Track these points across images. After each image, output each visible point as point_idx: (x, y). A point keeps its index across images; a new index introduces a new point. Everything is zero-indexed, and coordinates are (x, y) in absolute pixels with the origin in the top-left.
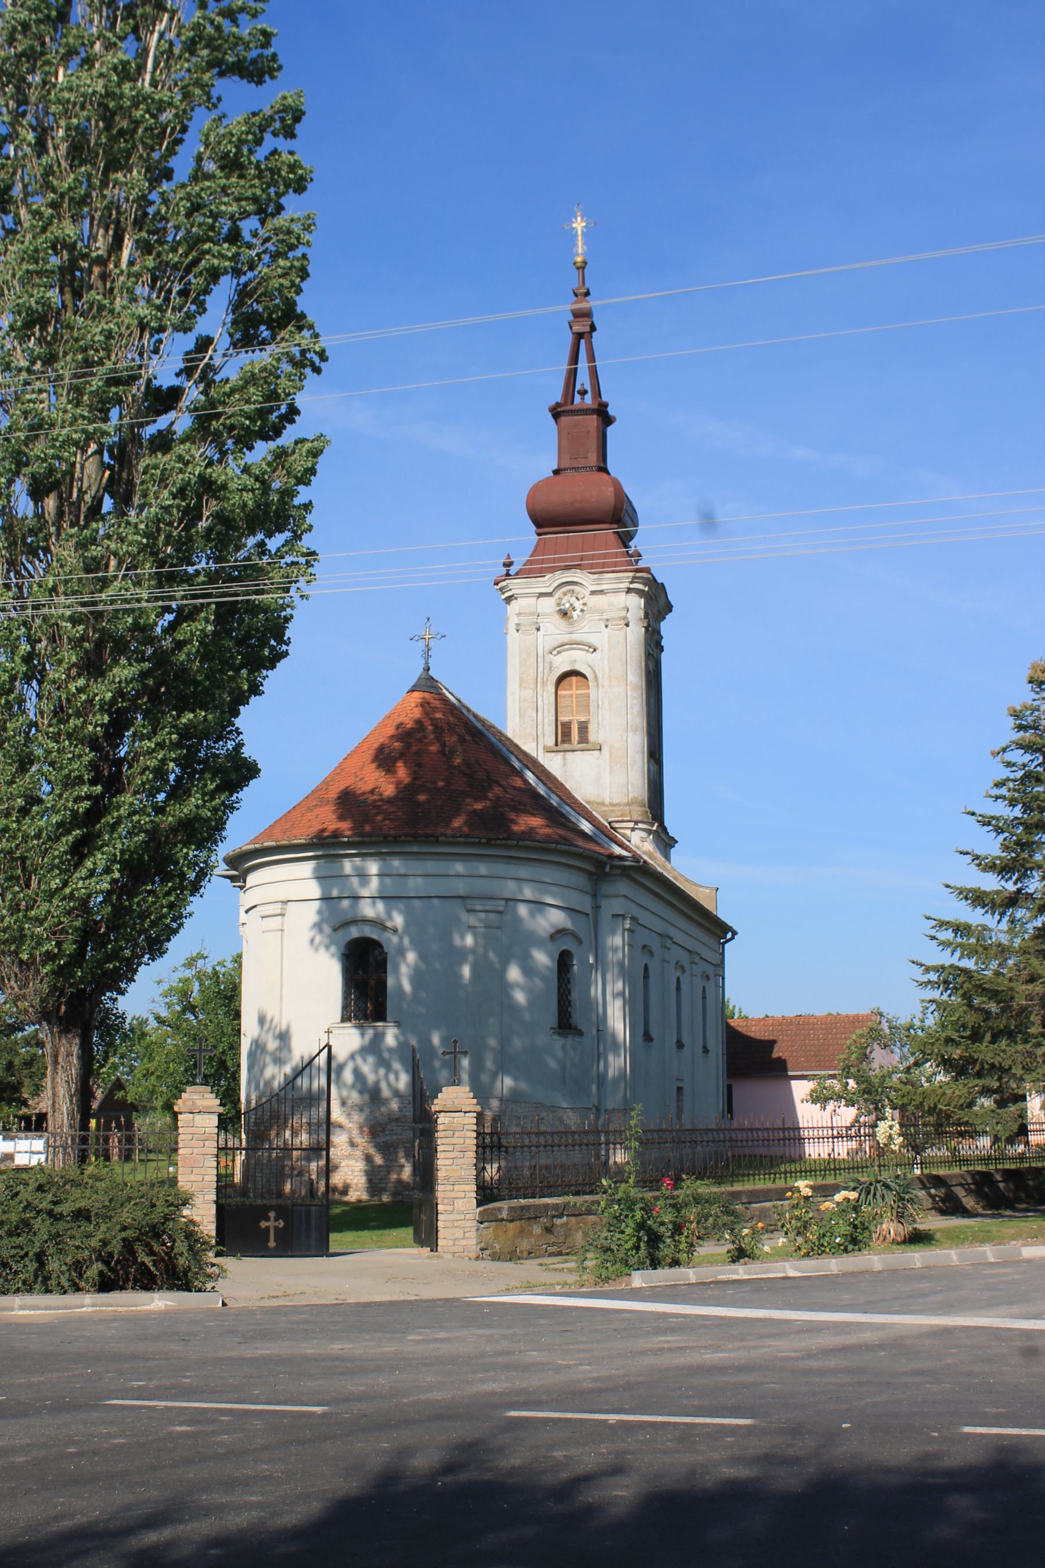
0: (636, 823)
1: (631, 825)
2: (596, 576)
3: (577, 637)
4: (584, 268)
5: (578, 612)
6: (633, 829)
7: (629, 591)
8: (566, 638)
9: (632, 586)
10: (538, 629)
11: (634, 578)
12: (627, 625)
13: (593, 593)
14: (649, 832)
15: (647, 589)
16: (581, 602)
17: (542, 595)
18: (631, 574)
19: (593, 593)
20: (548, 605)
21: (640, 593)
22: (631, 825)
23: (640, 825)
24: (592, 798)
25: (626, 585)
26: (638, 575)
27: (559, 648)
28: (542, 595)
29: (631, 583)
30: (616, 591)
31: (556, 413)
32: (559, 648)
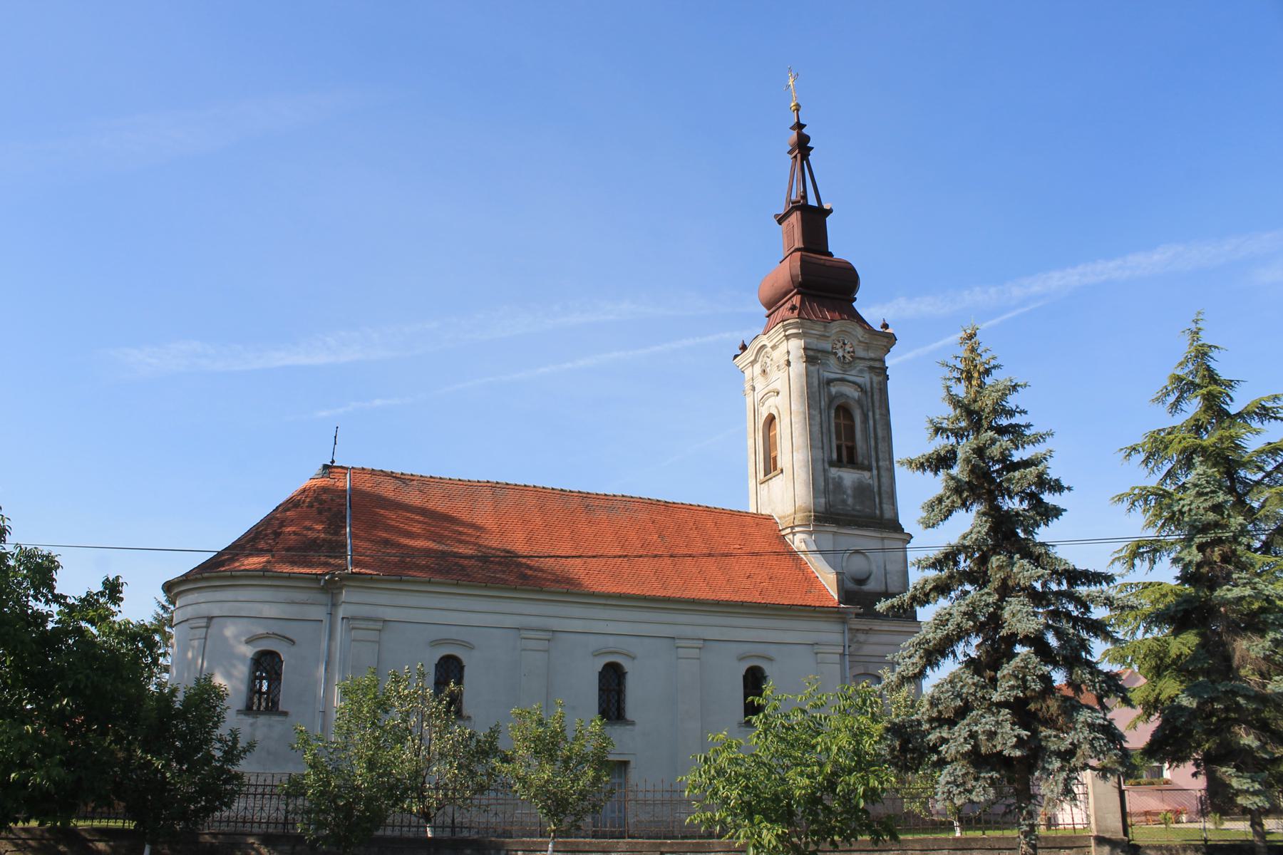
0: (792, 528)
1: (789, 530)
3: (770, 388)
6: (794, 534)
7: (787, 337)
8: (766, 391)
10: (754, 389)
12: (789, 363)
13: (774, 347)
14: (810, 533)
17: (753, 363)
19: (774, 347)
20: (758, 368)
21: (795, 335)
22: (789, 530)
23: (797, 529)
24: (782, 514)
27: (763, 400)
28: (753, 363)
31: (780, 222)
32: (763, 400)
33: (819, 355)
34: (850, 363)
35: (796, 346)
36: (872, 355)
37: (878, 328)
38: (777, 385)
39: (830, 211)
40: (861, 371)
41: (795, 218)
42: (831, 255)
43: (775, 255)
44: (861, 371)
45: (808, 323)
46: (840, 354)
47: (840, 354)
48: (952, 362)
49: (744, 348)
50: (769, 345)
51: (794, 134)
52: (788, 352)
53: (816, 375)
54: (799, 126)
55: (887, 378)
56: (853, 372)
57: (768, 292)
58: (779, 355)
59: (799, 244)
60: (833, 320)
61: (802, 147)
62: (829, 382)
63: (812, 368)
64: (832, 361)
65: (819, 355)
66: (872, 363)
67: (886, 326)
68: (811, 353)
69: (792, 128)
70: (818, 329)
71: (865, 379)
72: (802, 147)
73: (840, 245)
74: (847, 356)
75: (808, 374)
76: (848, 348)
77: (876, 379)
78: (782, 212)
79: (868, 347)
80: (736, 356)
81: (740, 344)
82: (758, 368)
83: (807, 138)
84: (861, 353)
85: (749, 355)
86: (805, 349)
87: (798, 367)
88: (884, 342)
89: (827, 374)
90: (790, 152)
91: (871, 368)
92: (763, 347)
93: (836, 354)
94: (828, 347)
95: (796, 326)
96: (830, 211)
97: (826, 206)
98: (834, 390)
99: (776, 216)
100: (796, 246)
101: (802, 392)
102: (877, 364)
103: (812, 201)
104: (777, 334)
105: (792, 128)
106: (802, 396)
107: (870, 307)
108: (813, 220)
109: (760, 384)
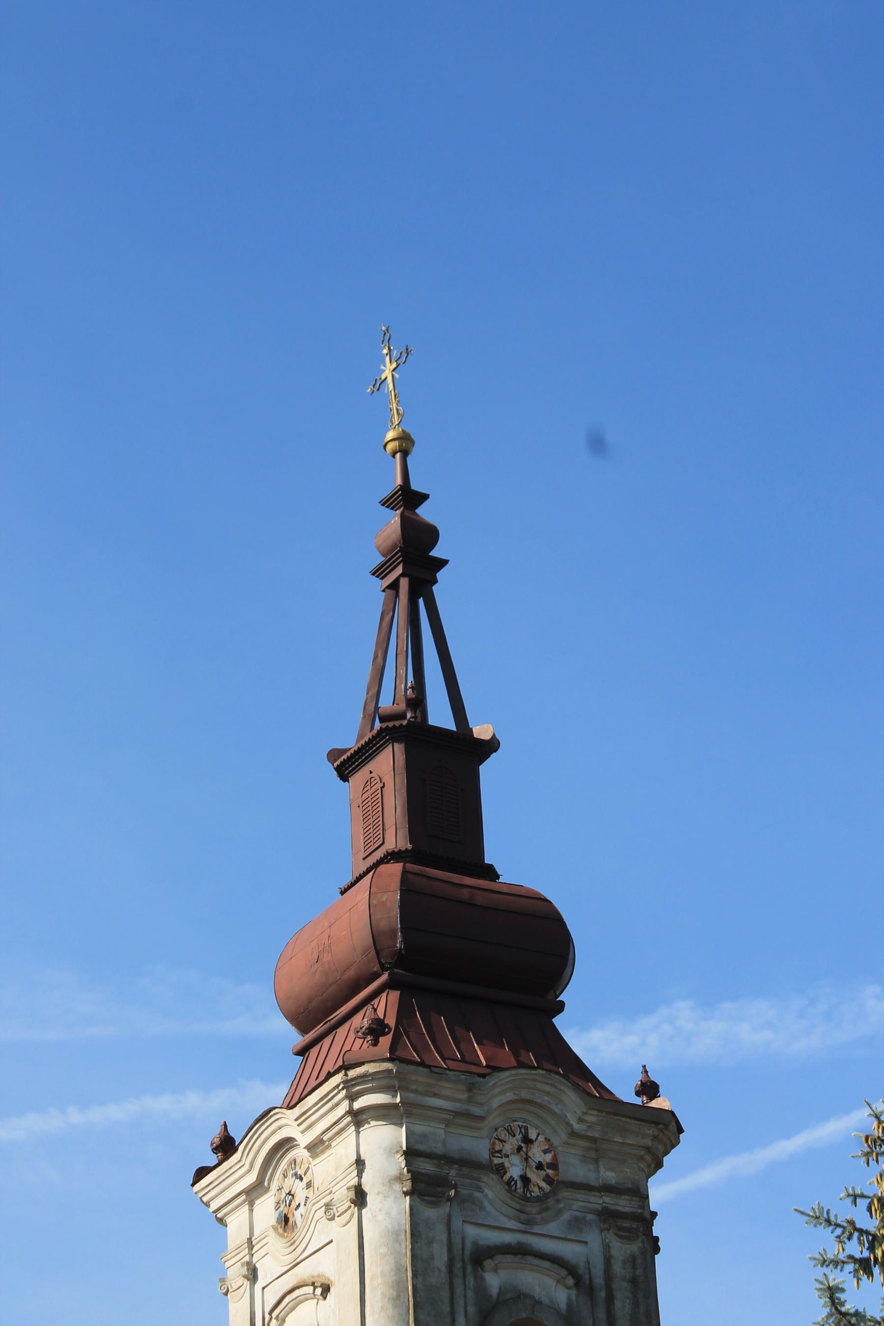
2: (297, 1111)
3: (304, 1271)
4: (405, 453)
5: (302, 1209)
7: (358, 1118)
9: (357, 1105)
10: (252, 1274)
11: (347, 1084)
15: (398, 1100)
16: (305, 1181)
18: (337, 1079)
19: (316, 1147)
20: (266, 1209)
21: (382, 1113)
25: (344, 1106)
26: (352, 1073)
29: (352, 1098)
30: (336, 1130)
31: (344, 771)
33: (453, 1173)
34: (542, 1199)
35: (383, 1143)
36: (609, 1176)
37: (627, 1094)
38: (321, 1266)
39: (490, 746)
40: (577, 1224)
41: (388, 764)
42: (491, 873)
43: (322, 870)
44: (577, 1224)
45: (420, 1076)
46: (515, 1171)
47: (515, 1171)
48: (844, 1212)
49: (226, 1146)
50: (303, 1140)
51: (393, 520)
52: (360, 1164)
53: (440, 1234)
54: (408, 498)
55: (654, 1246)
56: (552, 1228)
57: (304, 977)
58: (331, 1171)
59: (396, 838)
60: (494, 1068)
61: (415, 560)
62: (481, 1256)
63: (430, 1213)
64: (491, 1192)
65: (453, 1173)
66: (608, 1200)
67: (649, 1089)
68: (426, 1167)
69: (389, 503)
70: (447, 1096)
71: (586, 1249)
72: (415, 560)
73: (521, 843)
74: (536, 1178)
75: (417, 1231)
76: (537, 1154)
77: (621, 1250)
78: (350, 742)
79: (595, 1148)
80: (201, 1173)
81: (214, 1134)
82: (266, 1209)
83: (431, 535)
84: (575, 1168)
85: (240, 1171)
86: (410, 1154)
87: (389, 1209)
88: (646, 1135)
89: (472, 1232)
90: (380, 572)
91: (607, 1216)
92: (286, 1144)
93: (501, 1170)
94: (480, 1148)
95: (382, 1083)
96: (490, 746)
97: (481, 731)
98: (493, 1281)
99: (333, 755)
100: (390, 845)
101: (399, 1286)
102: (624, 1204)
103: (440, 715)
104: (328, 1106)
105: (389, 503)
106: (397, 1299)
107: (604, 1035)
108: (438, 769)
109: (272, 1259)
